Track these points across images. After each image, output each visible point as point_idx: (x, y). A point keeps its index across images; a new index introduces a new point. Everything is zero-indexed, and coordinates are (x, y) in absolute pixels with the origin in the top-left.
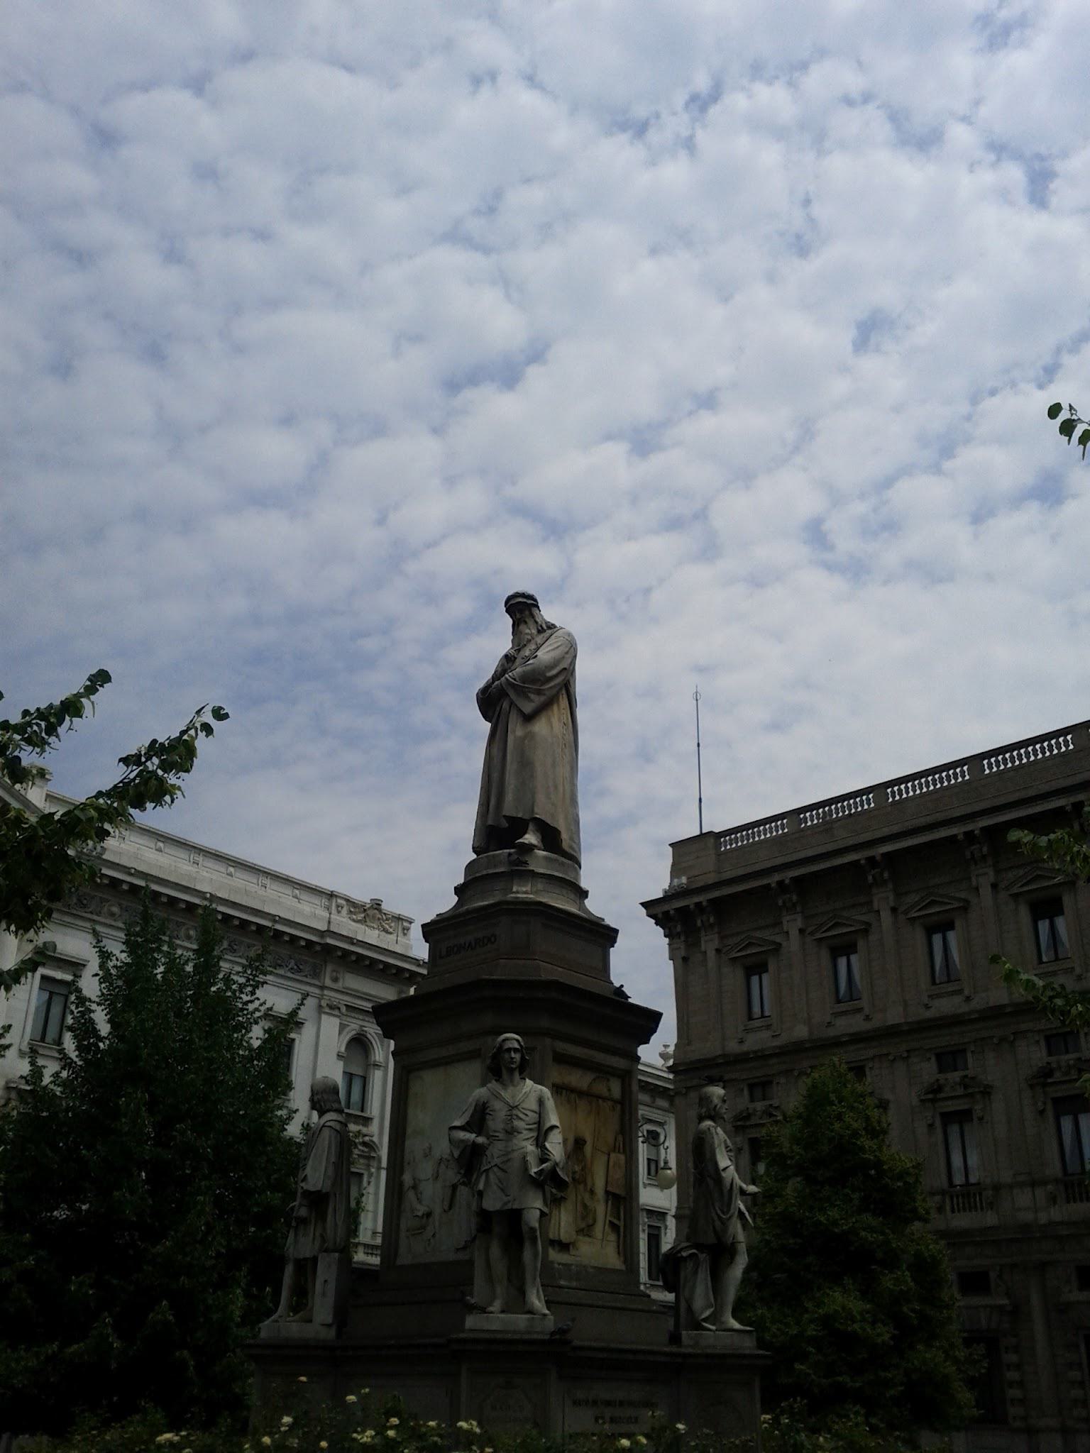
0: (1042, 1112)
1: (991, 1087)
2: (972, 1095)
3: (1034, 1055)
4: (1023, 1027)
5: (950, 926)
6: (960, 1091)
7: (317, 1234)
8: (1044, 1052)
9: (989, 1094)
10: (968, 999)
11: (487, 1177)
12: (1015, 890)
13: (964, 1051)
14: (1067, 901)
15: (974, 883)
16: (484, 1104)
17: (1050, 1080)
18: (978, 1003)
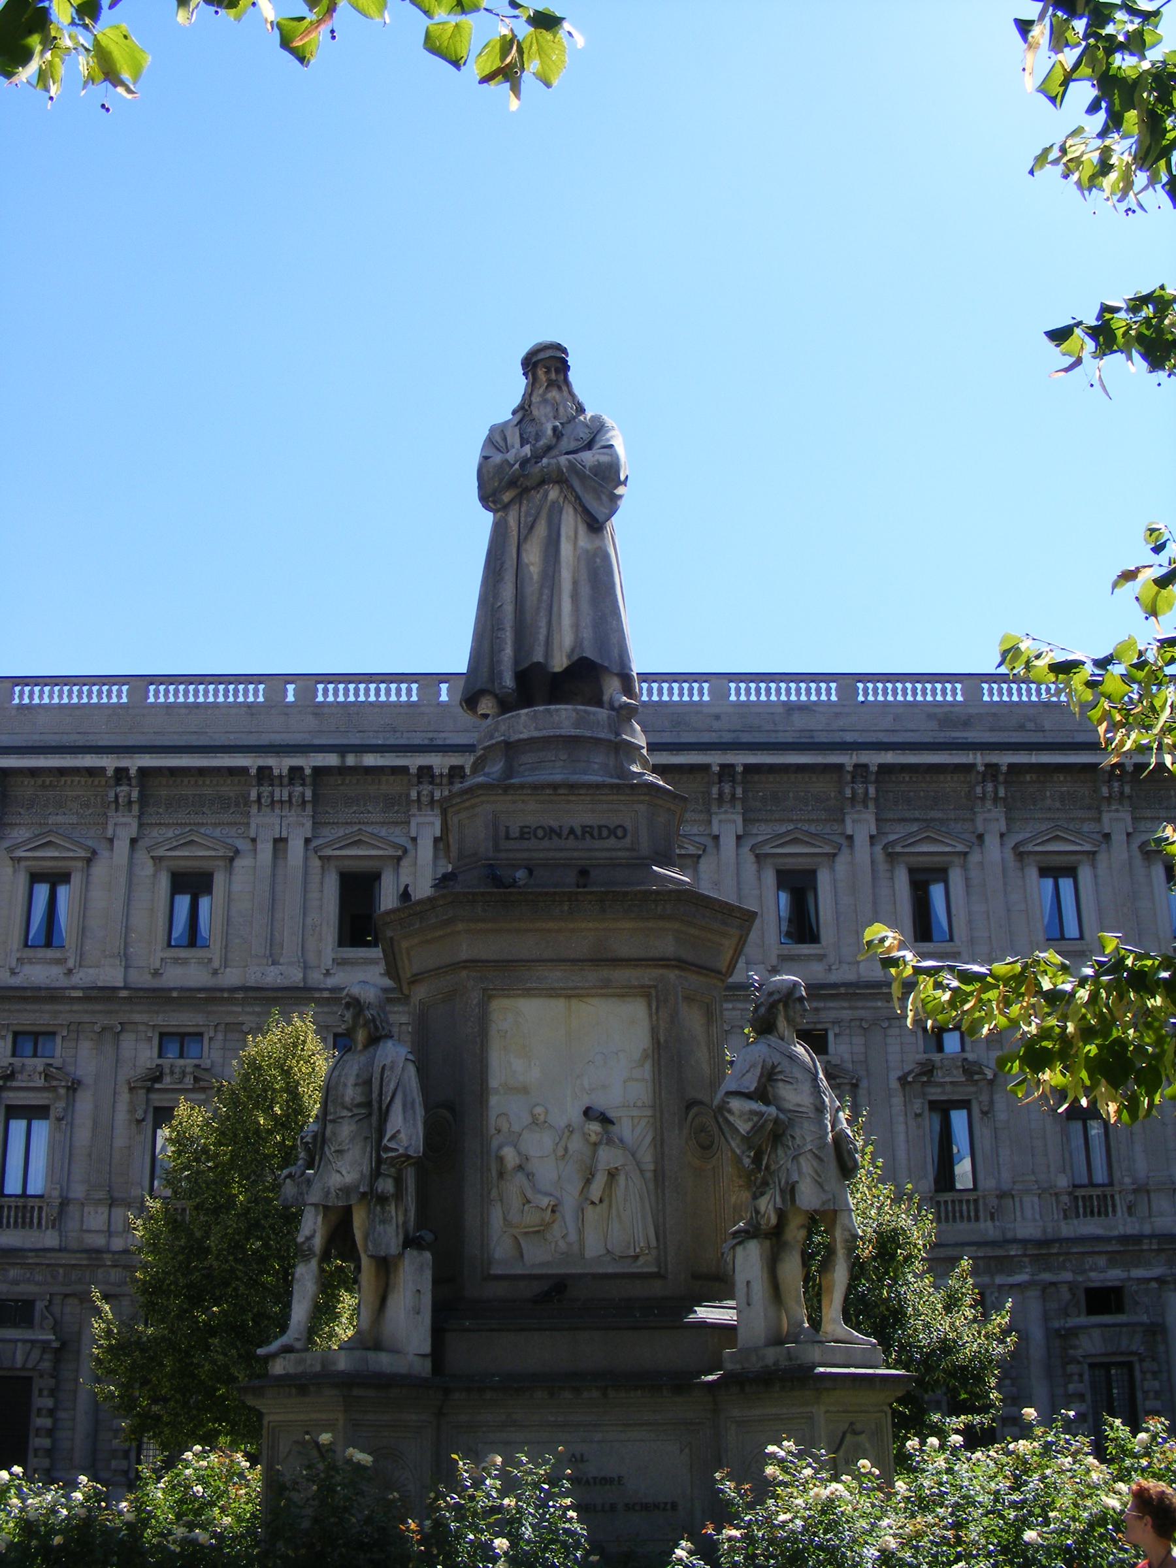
0: (139, 1122)
1: (79, 1082)
2: (54, 1089)
3: (142, 1054)
4: (137, 1018)
5: (65, 878)
6: (40, 1082)
7: (401, 1220)
8: (156, 1050)
9: (75, 1090)
10: (70, 972)
11: (799, 1164)
12: (160, 852)
13: (54, 1034)
14: (219, 880)
15: (109, 834)
16: (774, 1067)
17: (157, 1086)
18: (84, 977)
